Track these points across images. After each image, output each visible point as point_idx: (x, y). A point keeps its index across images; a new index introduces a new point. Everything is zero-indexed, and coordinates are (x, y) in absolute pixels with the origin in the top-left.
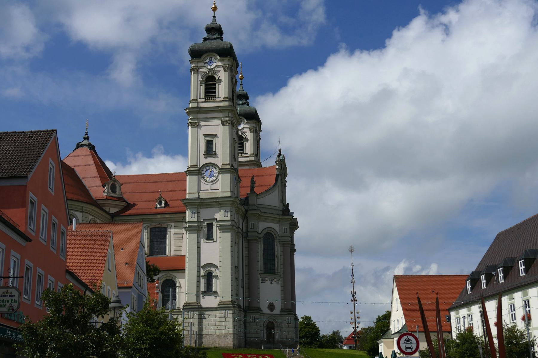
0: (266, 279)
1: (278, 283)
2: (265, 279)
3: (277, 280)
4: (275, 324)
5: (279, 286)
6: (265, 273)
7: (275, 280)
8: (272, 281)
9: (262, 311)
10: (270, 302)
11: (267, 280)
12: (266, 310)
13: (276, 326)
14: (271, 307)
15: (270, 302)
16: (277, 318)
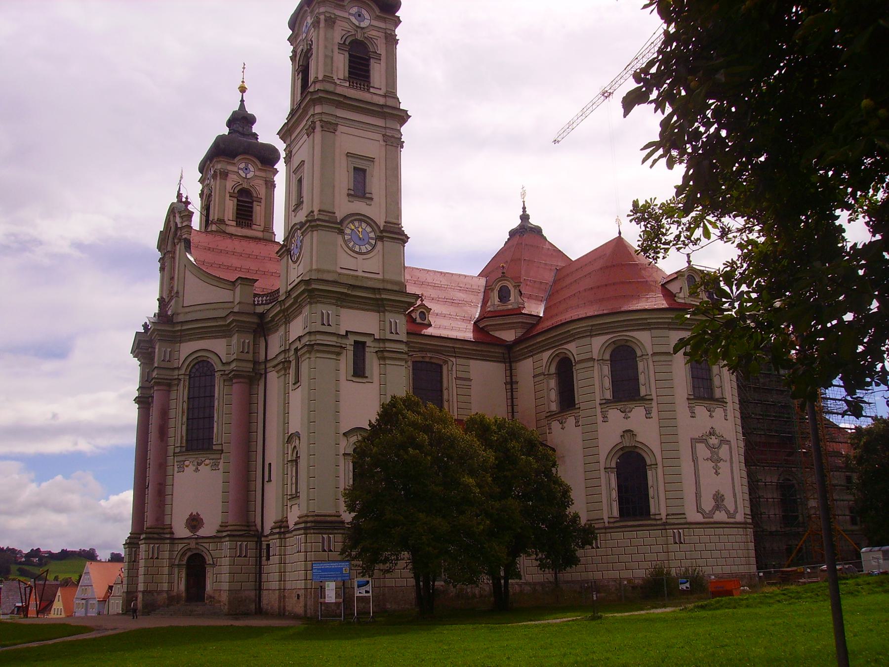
0: (187, 463)
1: (215, 466)
2: (184, 464)
3: (212, 461)
4: (206, 558)
5: (221, 470)
6: (192, 450)
7: (207, 462)
8: (199, 464)
9: (172, 533)
10: (192, 513)
11: (187, 466)
12: (181, 530)
13: (208, 562)
14: (194, 522)
15: (192, 513)
16: (206, 545)
